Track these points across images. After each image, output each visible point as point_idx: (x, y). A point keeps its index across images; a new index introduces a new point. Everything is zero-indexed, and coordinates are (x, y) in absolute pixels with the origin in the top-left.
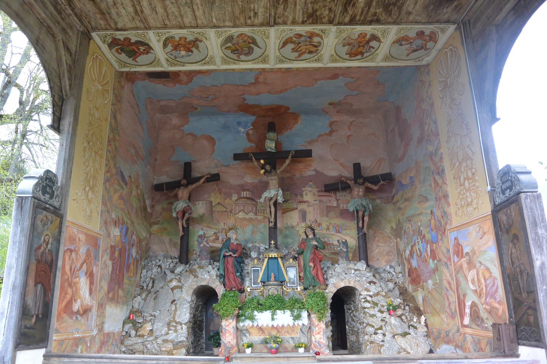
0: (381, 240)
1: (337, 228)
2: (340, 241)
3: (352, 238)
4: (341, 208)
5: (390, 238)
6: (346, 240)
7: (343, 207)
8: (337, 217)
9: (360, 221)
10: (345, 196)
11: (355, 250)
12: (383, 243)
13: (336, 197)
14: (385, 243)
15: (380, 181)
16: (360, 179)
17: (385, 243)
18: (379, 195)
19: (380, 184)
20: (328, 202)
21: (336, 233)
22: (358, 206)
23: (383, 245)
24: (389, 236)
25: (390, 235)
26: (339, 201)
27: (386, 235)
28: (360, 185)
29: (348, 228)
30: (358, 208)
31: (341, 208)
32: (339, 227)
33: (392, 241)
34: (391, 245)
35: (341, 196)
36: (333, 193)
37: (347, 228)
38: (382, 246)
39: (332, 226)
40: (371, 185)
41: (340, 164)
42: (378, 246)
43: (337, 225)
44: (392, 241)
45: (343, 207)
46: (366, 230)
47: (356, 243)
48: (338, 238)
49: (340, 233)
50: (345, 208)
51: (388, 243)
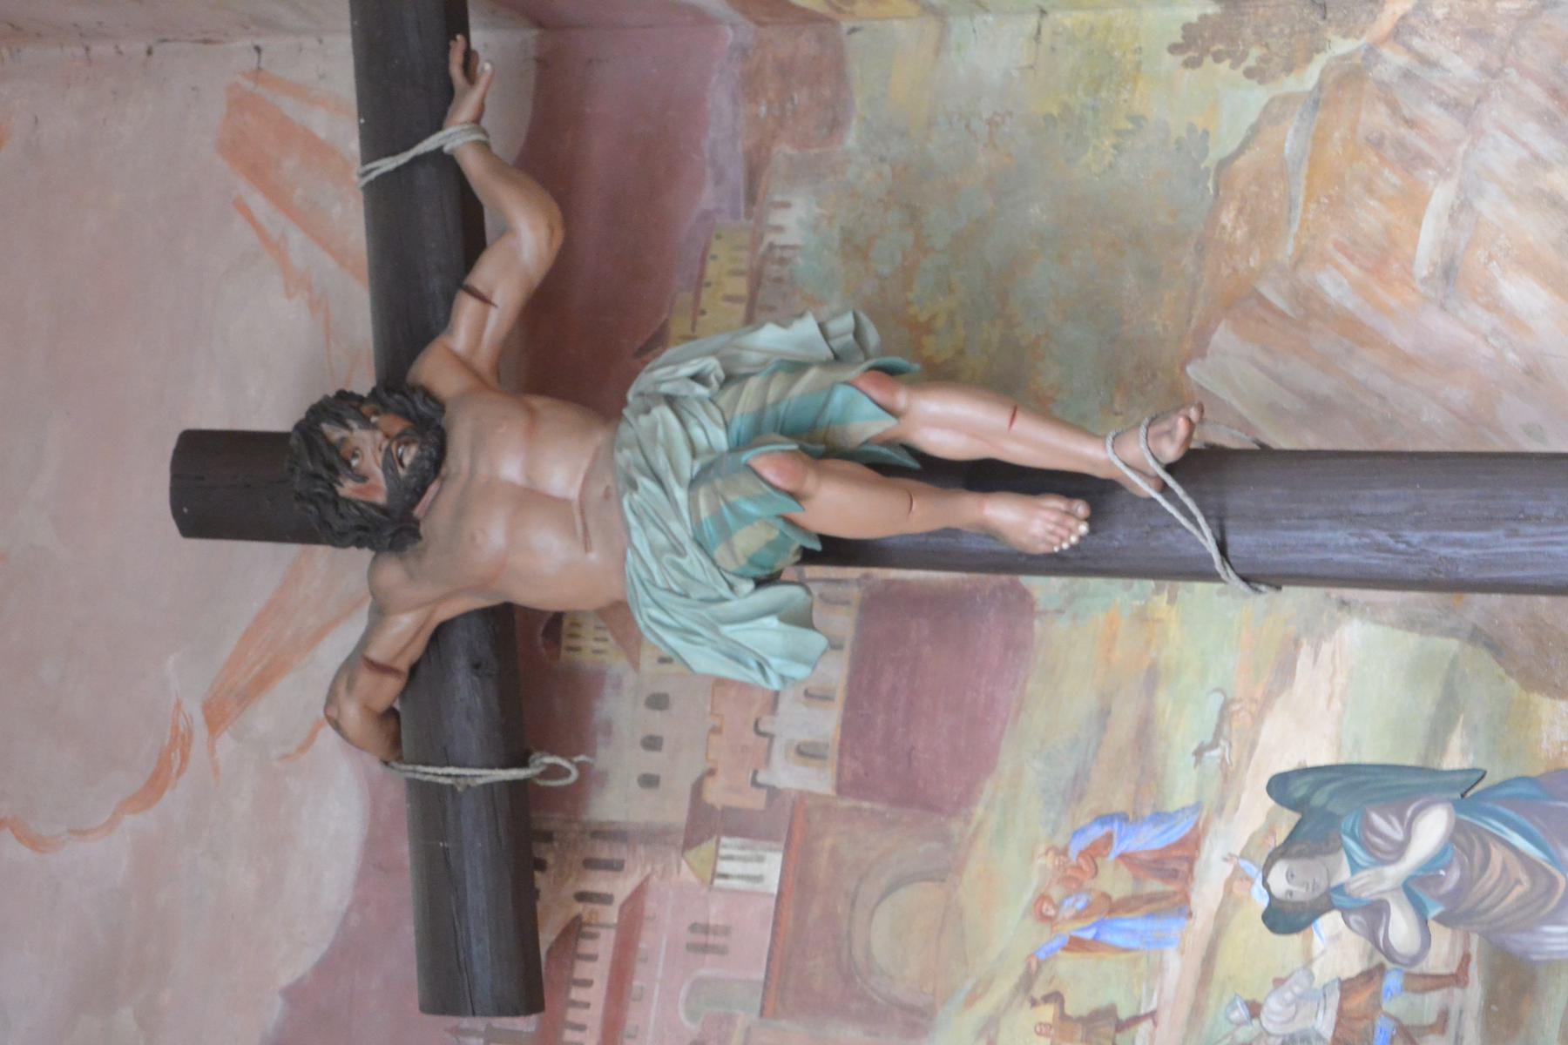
0: (1371, 217)
1: (1115, 882)
2: (1279, 880)
3: (1285, 669)
4: (818, 781)
5: (1350, 76)
6: (1280, 786)
7: (807, 753)
8: (943, 872)
9: (990, 533)
10: (658, 702)
11: (1491, 643)
12: (1414, 202)
13: (654, 836)
14: (1412, 160)
15: (445, 162)
16: (336, 462)
17: (1412, 160)
18: (708, 197)
19: (473, 166)
20: (708, 968)
21: (1181, 906)
22: (725, 533)
23: (1441, 196)
24: (1317, 101)
25: (1310, 76)
26: (716, 794)
27: (1291, 138)
28: (435, 462)
29: (1125, 716)
30: (750, 540)
31: (818, 781)
32: (1094, 853)
33: (1394, 59)
34: (1460, 66)
35: (651, 762)
36: (598, 882)
37: (1125, 716)
38: (1462, 207)
39: (1067, 965)
40: (467, 308)
41: (217, 716)
42: (1448, 272)
43: (1072, 879)
44: (1394, 59)
45: (807, 753)
46: (1137, 448)
47: (1372, 614)
48: (1249, 926)
49: (1189, 848)
50: (826, 724)
51: (1432, 113)
